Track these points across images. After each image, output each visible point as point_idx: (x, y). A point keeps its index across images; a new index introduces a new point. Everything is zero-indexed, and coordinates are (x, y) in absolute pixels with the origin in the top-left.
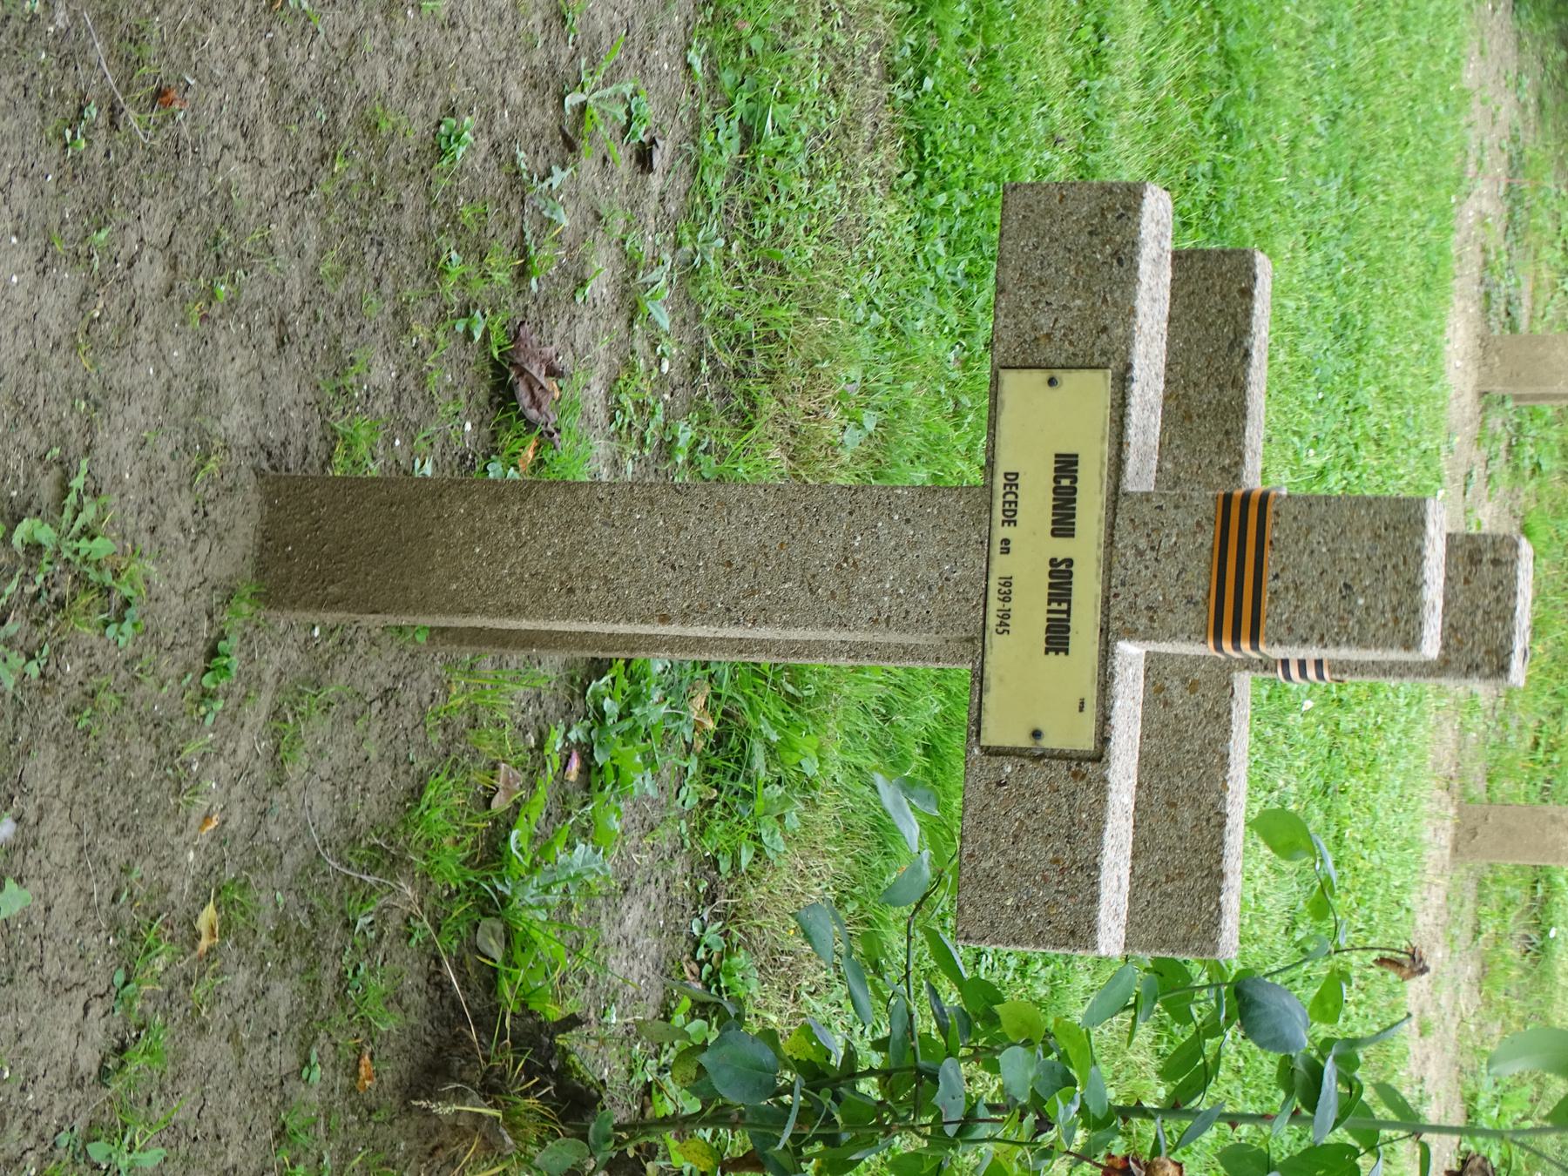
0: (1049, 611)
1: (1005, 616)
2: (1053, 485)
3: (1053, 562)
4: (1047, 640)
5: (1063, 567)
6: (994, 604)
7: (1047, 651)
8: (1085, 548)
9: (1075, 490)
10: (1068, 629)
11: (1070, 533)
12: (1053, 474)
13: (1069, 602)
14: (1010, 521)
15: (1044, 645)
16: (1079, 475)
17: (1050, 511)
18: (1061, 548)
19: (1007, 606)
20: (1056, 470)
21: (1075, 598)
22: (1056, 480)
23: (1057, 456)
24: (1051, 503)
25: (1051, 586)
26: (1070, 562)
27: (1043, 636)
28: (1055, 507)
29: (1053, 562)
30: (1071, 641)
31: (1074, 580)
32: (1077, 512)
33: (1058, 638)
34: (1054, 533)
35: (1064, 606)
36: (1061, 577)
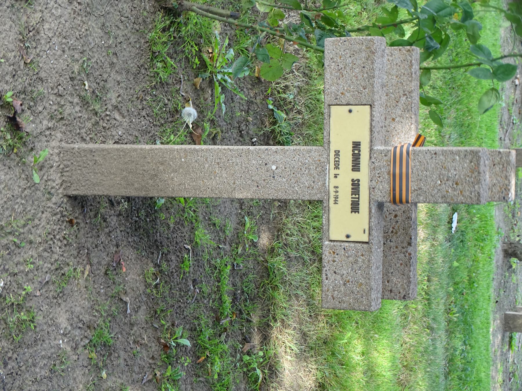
0: (352, 198)
2: (352, 153)
3: (353, 180)
4: (352, 208)
5: (356, 182)
7: (352, 212)
9: (360, 155)
10: (359, 204)
11: (358, 170)
12: (352, 149)
13: (359, 194)
16: (361, 149)
18: (356, 175)
20: (353, 147)
21: (360, 193)
22: (353, 151)
23: (353, 142)
24: (351, 159)
25: (352, 189)
26: (358, 180)
27: (350, 207)
28: (353, 161)
29: (353, 180)
31: (360, 186)
32: (361, 162)
33: (355, 207)
34: (353, 170)
35: (357, 196)
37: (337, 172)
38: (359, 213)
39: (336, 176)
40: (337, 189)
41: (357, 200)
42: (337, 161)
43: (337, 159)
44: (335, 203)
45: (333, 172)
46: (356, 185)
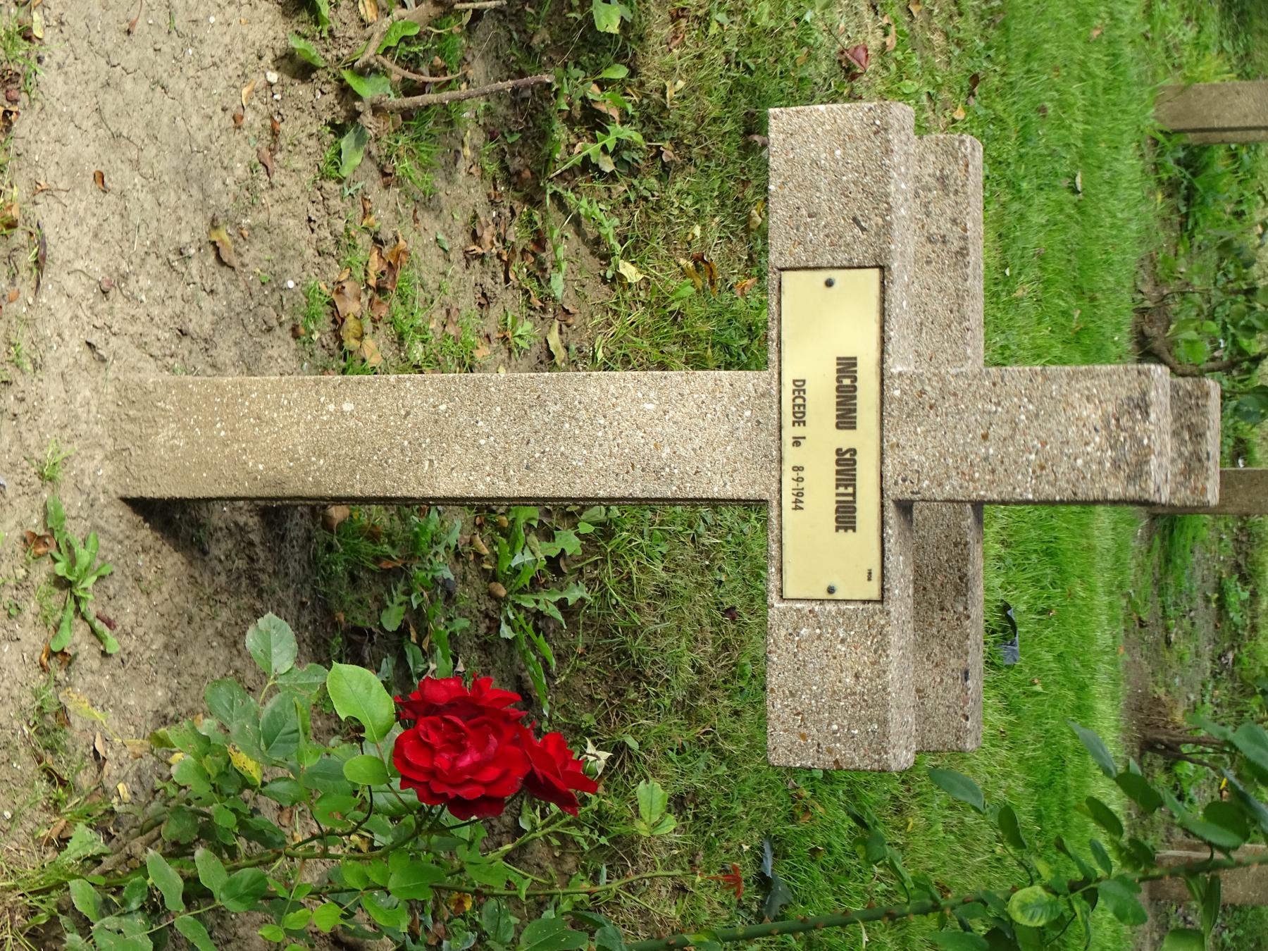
0: (838, 495)
2: (836, 384)
5: (848, 456)
7: (837, 529)
8: (864, 440)
9: (855, 388)
12: (835, 375)
13: (854, 486)
15: (835, 524)
16: (858, 375)
17: (834, 407)
18: (846, 439)
20: (839, 371)
21: (858, 483)
22: (839, 380)
23: (838, 359)
24: (835, 400)
25: (838, 472)
27: (834, 516)
28: (838, 404)
30: (858, 520)
33: (846, 517)
34: (838, 426)
35: (850, 490)
37: (799, 430)
38: (854, 529)
39: (797, 442)
40: (801, 474)
41: (850, 498)
42: (799, 406)
43: (799, 401)
45: (789, 432)
46: (846, 464)
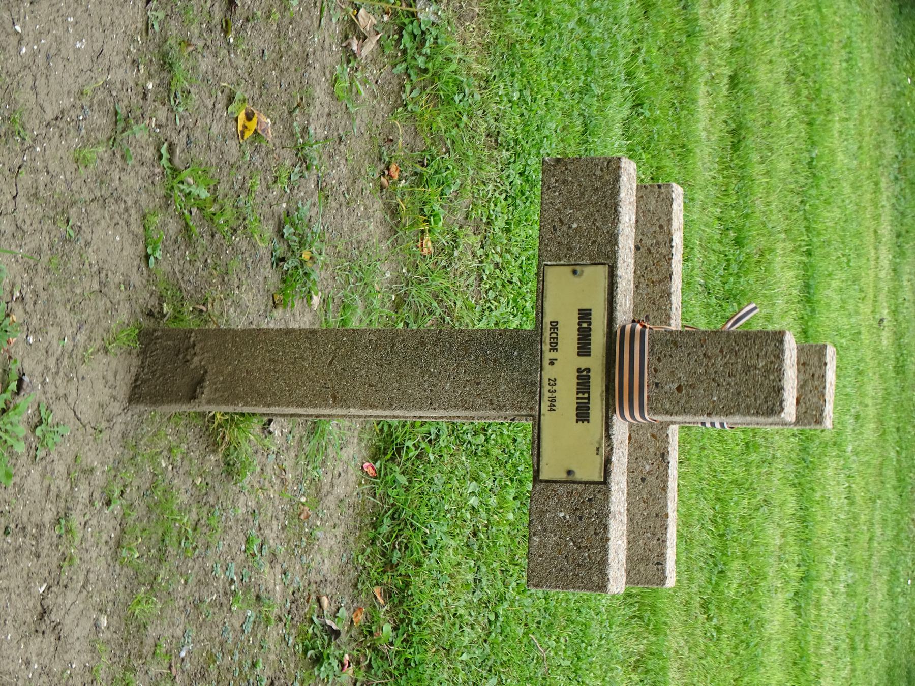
0: (578, 399)
1: (553, 401)
4: (577, 415)
5: (585, 373)
6: (546, 395)
8: (595, 362)
10: (589, 408)
11: (588, 354)
12: (577, 321)
13: (589, 393)
14: (554, 348)
15: (575, 418)
18: (584, 362)
19: (554, 395)
20: (579, 318)
22: (579, 324)
23: (579, 310)
26: (588, 370)
28: (579, 339)
29: (579, 370)
31: (591, 380)
33: (583, 414)
34: (579, 354)
35: (586, 395)
36: (583, 377)
42: (554, 338)
44: (551, 410)
45: (548, 355)
